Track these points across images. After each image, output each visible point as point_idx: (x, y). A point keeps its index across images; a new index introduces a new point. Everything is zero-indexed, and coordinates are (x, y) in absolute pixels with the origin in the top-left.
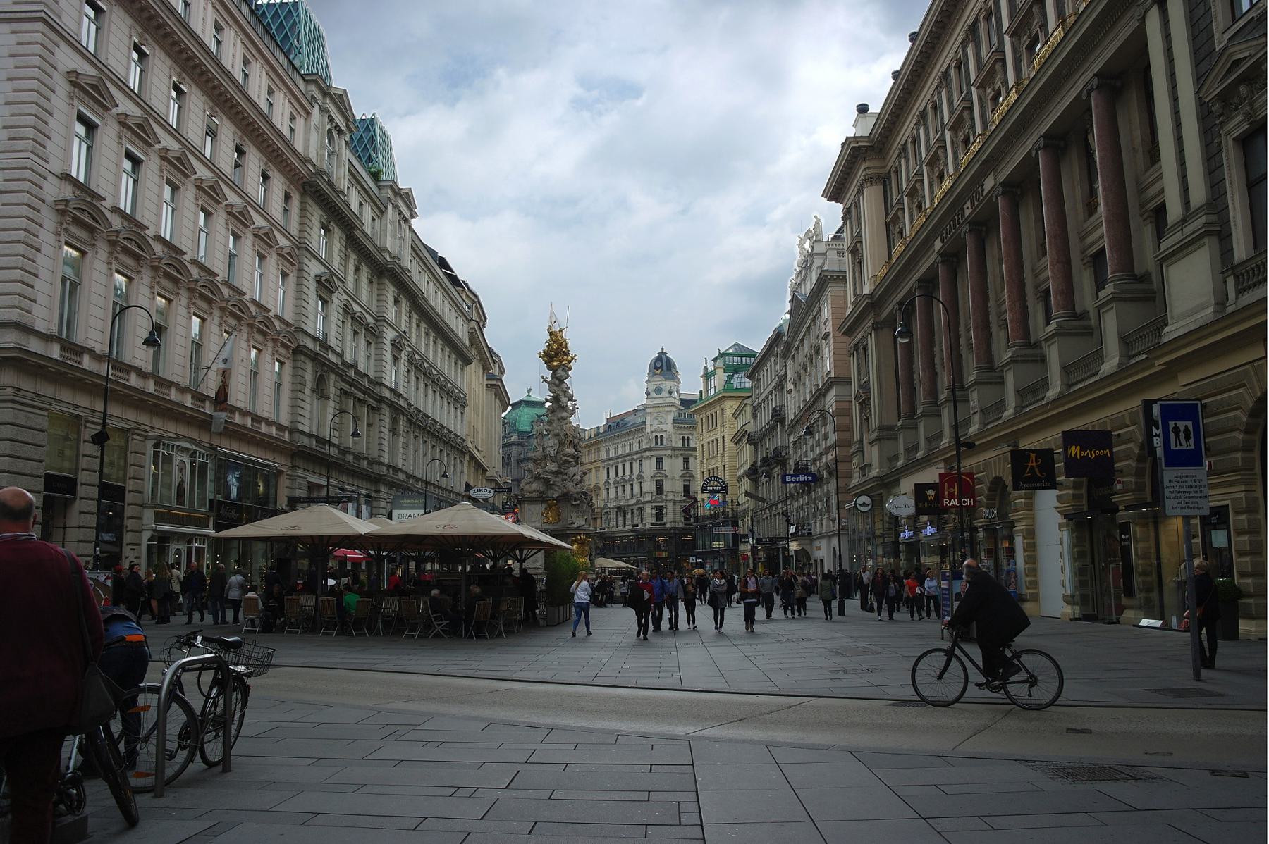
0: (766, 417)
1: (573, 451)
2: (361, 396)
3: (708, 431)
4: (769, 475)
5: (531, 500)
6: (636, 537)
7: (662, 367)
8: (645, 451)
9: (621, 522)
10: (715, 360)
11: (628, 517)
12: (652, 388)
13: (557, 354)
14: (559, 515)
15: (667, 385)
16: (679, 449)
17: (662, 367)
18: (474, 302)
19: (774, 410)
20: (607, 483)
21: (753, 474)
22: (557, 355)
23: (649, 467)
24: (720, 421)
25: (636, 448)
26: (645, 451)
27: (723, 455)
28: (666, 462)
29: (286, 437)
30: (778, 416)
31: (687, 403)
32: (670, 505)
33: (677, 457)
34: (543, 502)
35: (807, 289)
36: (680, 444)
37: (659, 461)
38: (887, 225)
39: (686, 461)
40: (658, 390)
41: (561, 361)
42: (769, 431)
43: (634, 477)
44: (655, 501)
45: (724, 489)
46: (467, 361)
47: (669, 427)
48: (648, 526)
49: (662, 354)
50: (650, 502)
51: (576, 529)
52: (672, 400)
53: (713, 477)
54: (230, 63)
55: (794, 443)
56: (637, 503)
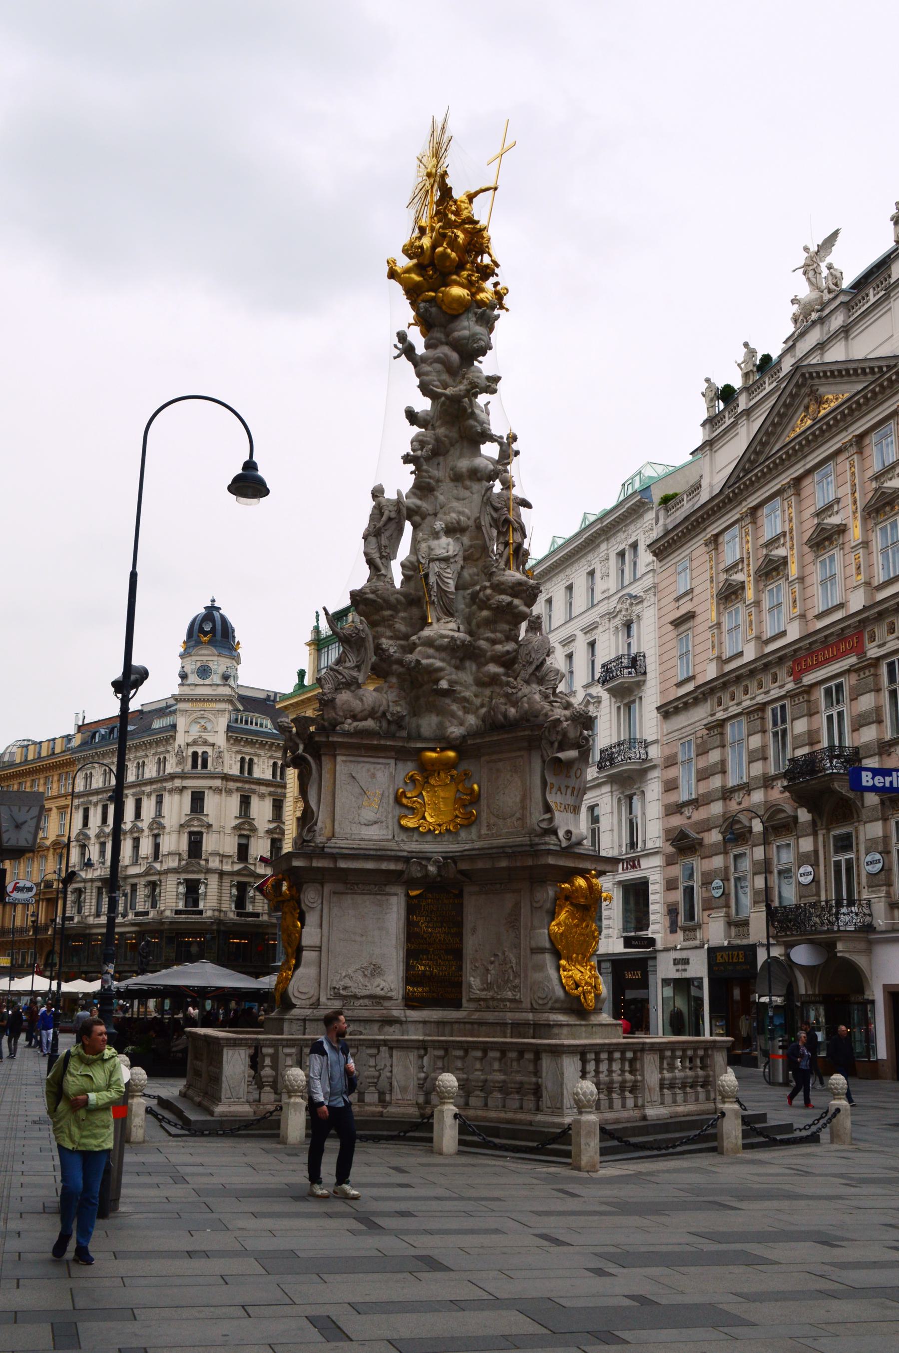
7: (213, 630)
14: (475, 799)
15: (219, 665)
23: (176, 808)
26: (172, 777)
28: (211, 803)
32: (213, 880)
33: (229, 792)
34: (402, 754)
36: (235, 771)
37: (198, 800)
39: (245, 802)
40: (204, 672)
44: (185, 870)
47: (220, 739)
49: (212, 611)
52: (226, 691)
56: (147, 873)
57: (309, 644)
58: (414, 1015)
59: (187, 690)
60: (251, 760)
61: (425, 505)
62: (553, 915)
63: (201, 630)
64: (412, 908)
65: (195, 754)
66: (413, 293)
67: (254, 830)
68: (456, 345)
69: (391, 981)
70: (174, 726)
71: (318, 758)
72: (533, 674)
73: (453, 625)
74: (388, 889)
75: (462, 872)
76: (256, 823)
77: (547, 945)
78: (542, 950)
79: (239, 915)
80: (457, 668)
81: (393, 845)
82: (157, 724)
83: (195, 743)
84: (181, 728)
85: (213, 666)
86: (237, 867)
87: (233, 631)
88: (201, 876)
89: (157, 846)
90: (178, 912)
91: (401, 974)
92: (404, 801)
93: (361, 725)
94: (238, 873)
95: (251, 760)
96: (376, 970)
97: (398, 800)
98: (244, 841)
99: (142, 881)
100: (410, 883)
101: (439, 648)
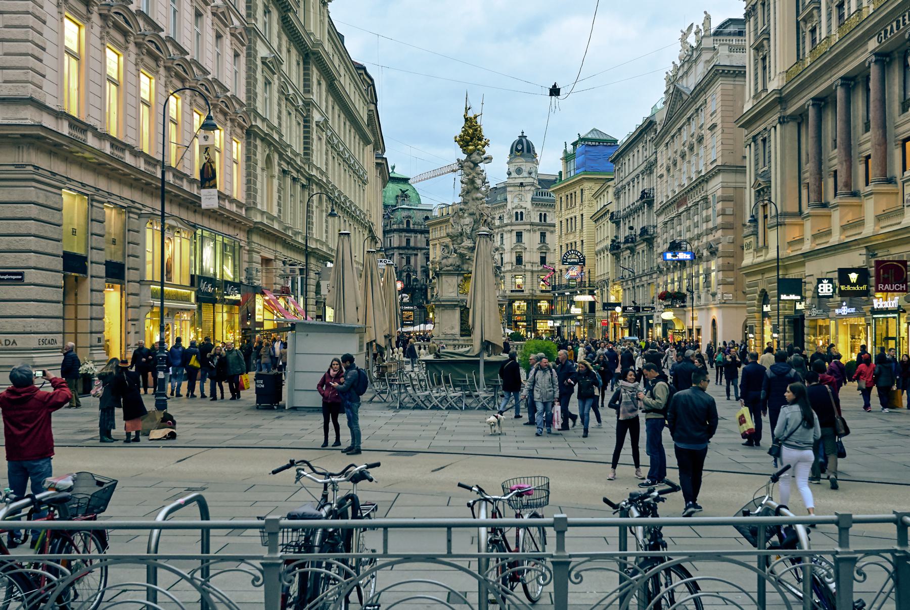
0: (632, 197)
2: (295, 174)
3: (567, 209)
4: (632, 250)
5: (449, 273)
7: (522, 149)
8: (506, 225)
10: (575, 144)
13: (472, 139)
15: (526, 167)
16: (538, 225)
17: (522, 149)
19: (643, 192)
21: (615, 248)
23: (509, 240)
26: (506, 225)
27: (581, 231)
28: (525, 236)
29: (243, 212)
30: (647, 199)
31: (546, 183)
33: (535, 231)
34: (458, 275)
35: (690, 83)
37: (519, 235)
38: (798, 23)
39: (543, 235)
40: (519, 171)
42: (634, 211)
45: (582, 262)
47: (529, 205)
52: (531, 180)
53: (571, 249)
55: (666, 223)
59: (511, 181)
61: (465, 207)
63: (517, 150)
65: (517, 213)
67: (548, 249)
68: (472, 162)
69: (457, 330)
76: (549, 246)
83: (516, 208)
85: (523, 168)
86: (541, 268)
90: (512, 291)
96: (453, 328)
100: (461, 307)
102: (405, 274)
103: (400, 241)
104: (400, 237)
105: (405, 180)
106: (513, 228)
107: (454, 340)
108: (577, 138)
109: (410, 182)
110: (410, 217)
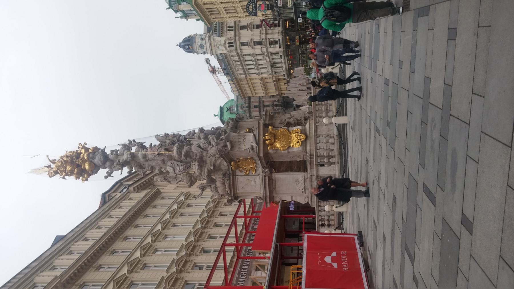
1: (175, 149)
6: (288, 55)
7: (188, 45)
8: (237, 53)
9: (280, 65)
10: (176, 12)
11: (277, 61)
12: (200, 50)
13: (79, 166)
15: (198, 42)
17: (188, 45)
18: (122, 184)
20: (258, 74)
22: (79, 164)
23: (246, 50)
24: (212, 6)
25: (236, 58)
26: (237, 53)
28: (244, 40)
31: (209, 30)
32: (269, 36)
33: (240, 34)
34: (234, 175)
36: (232, 32)
37: (243, 44)
39: (242, 28)
40: (202, 47)
41: (84, 161)
43: (253, 59)
46: (157, 194)
47: (223, 39)
48: (281, 49)
50: (267, 49)
51: (258, 143)
52: (207, 38)
54: (71, 261)
57: (187, 20)
58: (309, 171)
59: (209, 52)
60: (228, 27)
62: (277, 149)
64: (279, 171)
65: (229, 47)
66: (89, 175)
67: (251, 23)
69: (300, 176)
70: (221, 54)
71: (238, 197)
72: (205, 150)
73: (194, 166)
74: (273, 178)
75: (267, 164)
76: (249, 23)
77: (287, 151)
78: (289, 152)
79: (279, 26)
80: (206, 163)
81: (261, 176)
82: (220, 58)
83: (225, 47)
84: (221, 52)
86: (264, 28)
87: (186, 38)
88: (268, 40)
89: (259, 54)
90: (280, 47)
91: (297, 173)
92: (248, 173)
93: (227, 187)
94: (266, 28)
95: (228, 27)
96: (297, 181)
97: (247, 175)
98: (255, 27)
99: (271, 57)
100: (271, 173)
101: (201, 171)
102: (275, 108)
103: (256, 111)
104: (253, 111)
105: (222, 109)
106: (238, 48)
107: (311, 179)
108: (171, 10)
109: (222, 106)
110: (241, 106)
